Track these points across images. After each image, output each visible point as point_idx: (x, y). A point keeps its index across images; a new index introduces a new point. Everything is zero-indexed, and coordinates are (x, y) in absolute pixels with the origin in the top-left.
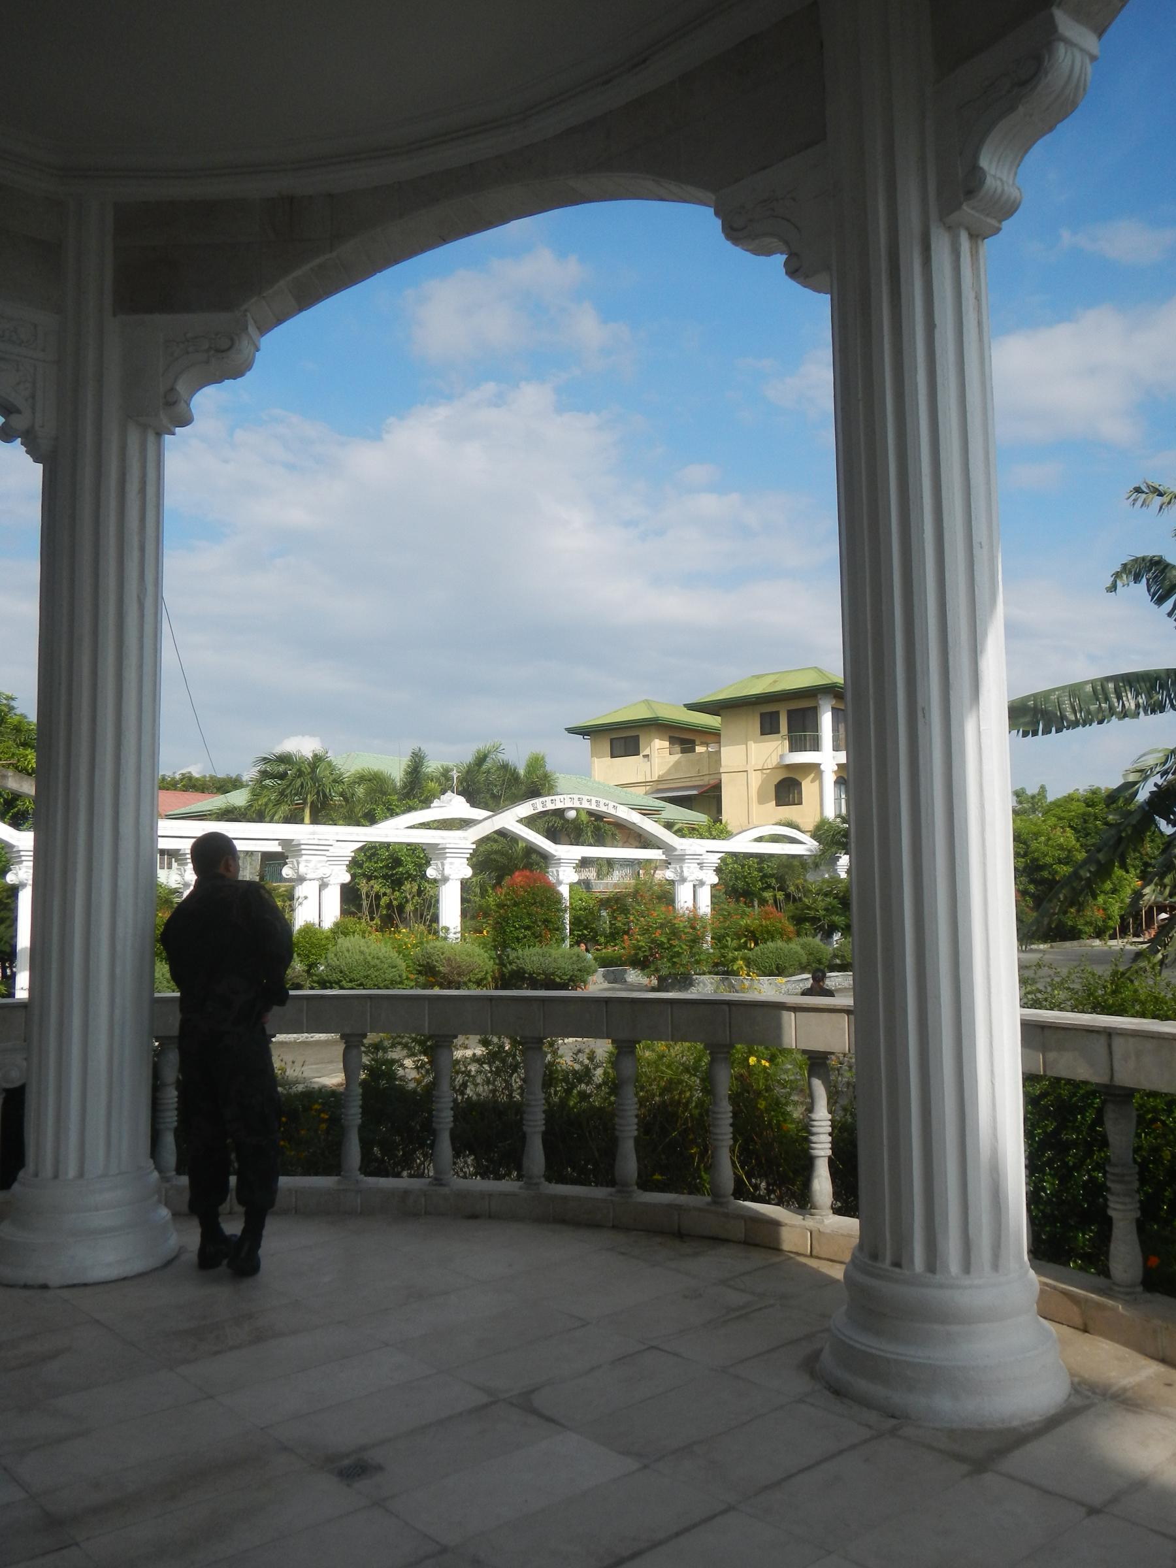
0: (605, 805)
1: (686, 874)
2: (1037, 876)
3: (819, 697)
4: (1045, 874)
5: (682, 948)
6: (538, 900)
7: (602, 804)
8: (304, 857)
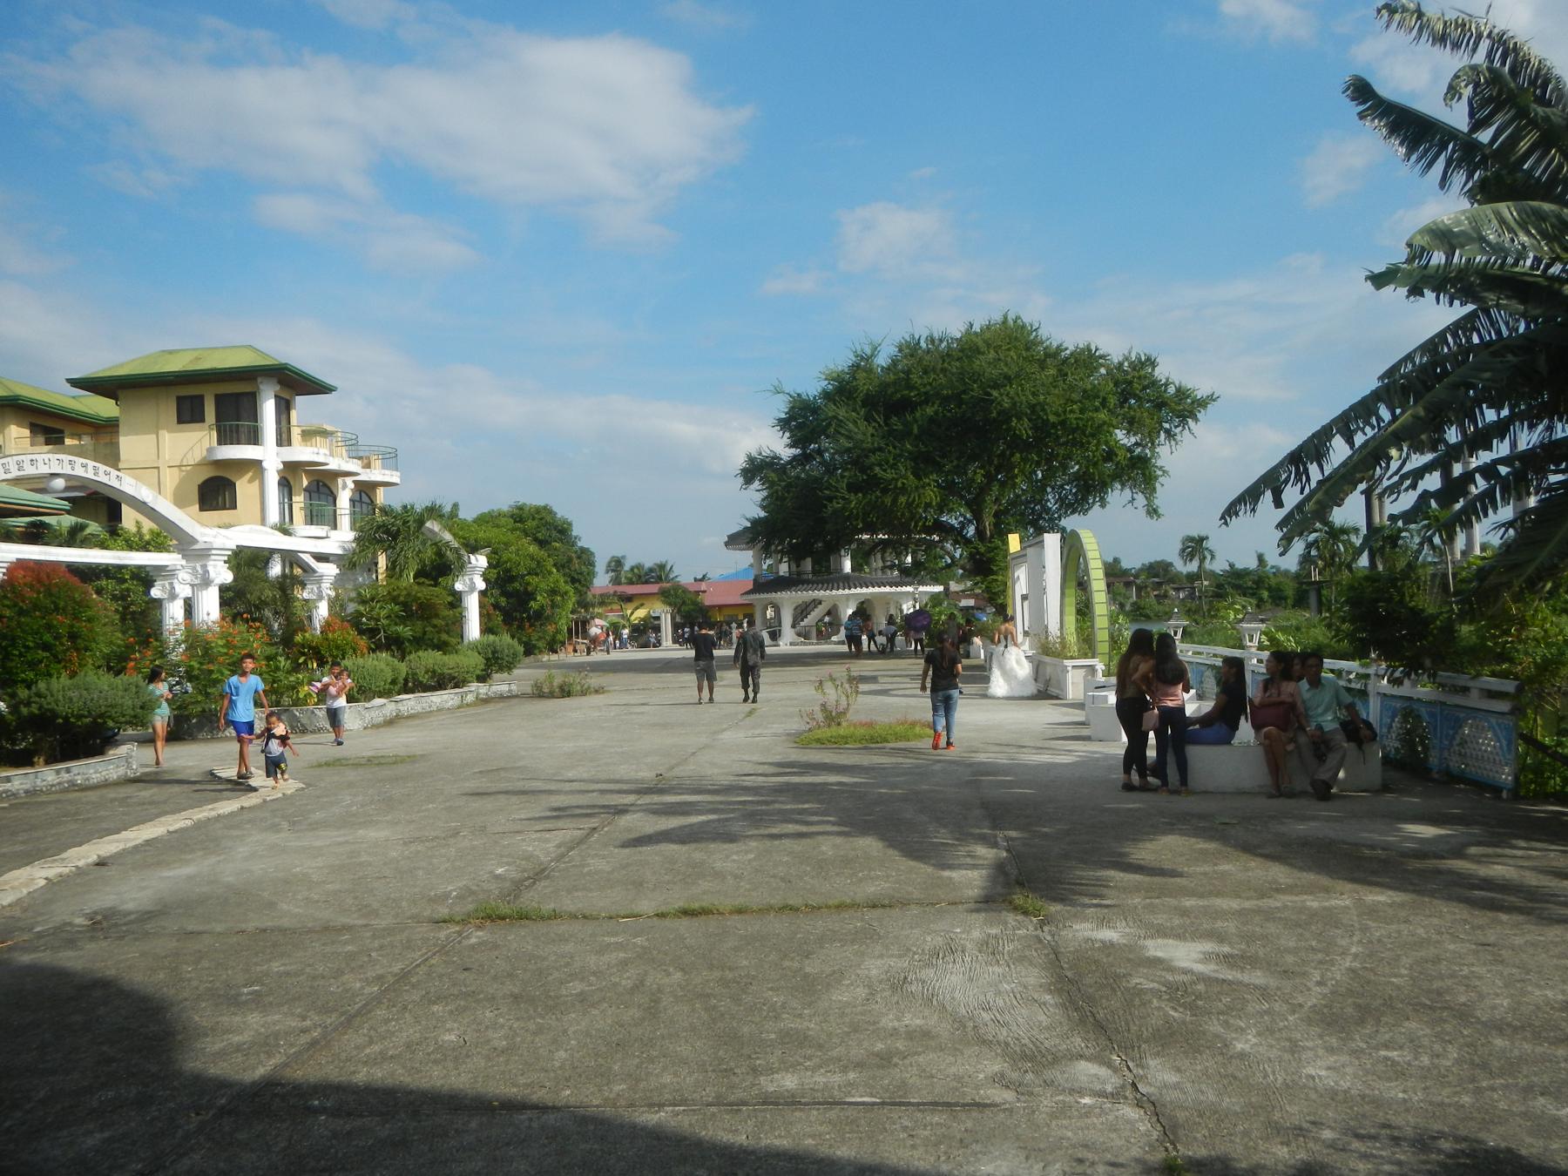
0: (106, 474)
1: (212, 575)
2: (510, 588)
3: (259, 380)
4: (516, 585)
5: (222, 674)
6: (62, 604)
7: (101, 473)
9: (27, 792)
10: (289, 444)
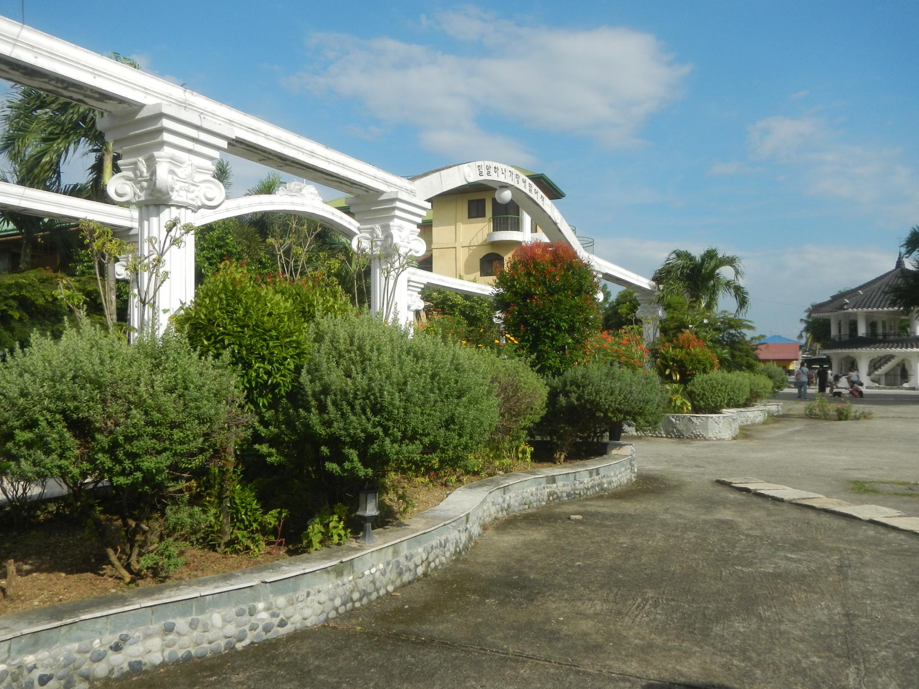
8: (167, 150)
9: (568, 495)
10: (536, 231)
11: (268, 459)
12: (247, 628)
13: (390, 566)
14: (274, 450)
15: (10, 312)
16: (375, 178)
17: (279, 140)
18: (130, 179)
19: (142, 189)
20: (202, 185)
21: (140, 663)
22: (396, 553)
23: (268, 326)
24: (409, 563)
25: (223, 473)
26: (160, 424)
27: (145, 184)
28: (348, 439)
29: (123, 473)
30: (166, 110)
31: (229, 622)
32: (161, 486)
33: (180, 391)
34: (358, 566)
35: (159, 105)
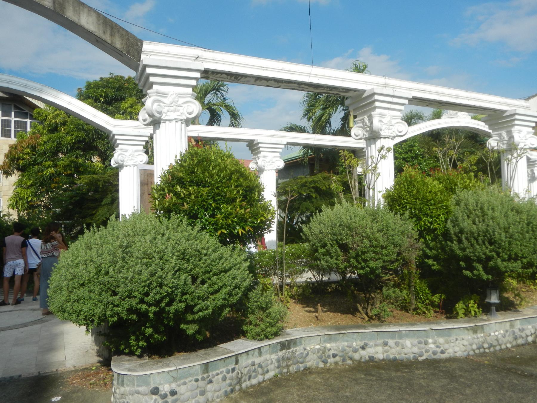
8: (378, 111)
11: (433, 267)
12: (424, 350)
13: (508, 333)
14: (435, 263)
15: (311, 194)
16: (500, 103)
17: (437, 93)
18: (361, 127)
19: (367, 131)
20: (396, 125)
21: (373, 357)
22: (512, 326)
23: (429, 198)
24: (522, 334)
25: (410, 273)
26: (377, 247)
27: (368, 129)
28: (475, 258)
29: (362, 268)
30: (376, 91)
31: (415, 346)
32: (378, 276)
33: (385, 231)
34: (486, 329)
35: (373, 89)
